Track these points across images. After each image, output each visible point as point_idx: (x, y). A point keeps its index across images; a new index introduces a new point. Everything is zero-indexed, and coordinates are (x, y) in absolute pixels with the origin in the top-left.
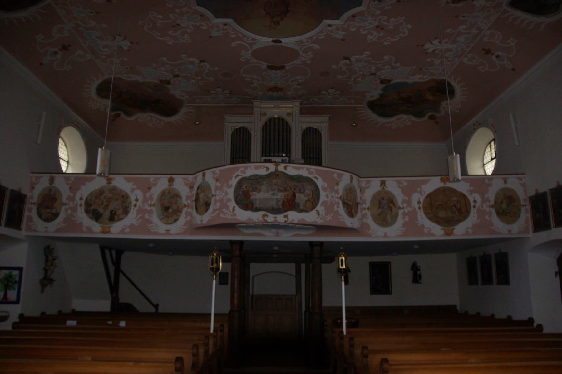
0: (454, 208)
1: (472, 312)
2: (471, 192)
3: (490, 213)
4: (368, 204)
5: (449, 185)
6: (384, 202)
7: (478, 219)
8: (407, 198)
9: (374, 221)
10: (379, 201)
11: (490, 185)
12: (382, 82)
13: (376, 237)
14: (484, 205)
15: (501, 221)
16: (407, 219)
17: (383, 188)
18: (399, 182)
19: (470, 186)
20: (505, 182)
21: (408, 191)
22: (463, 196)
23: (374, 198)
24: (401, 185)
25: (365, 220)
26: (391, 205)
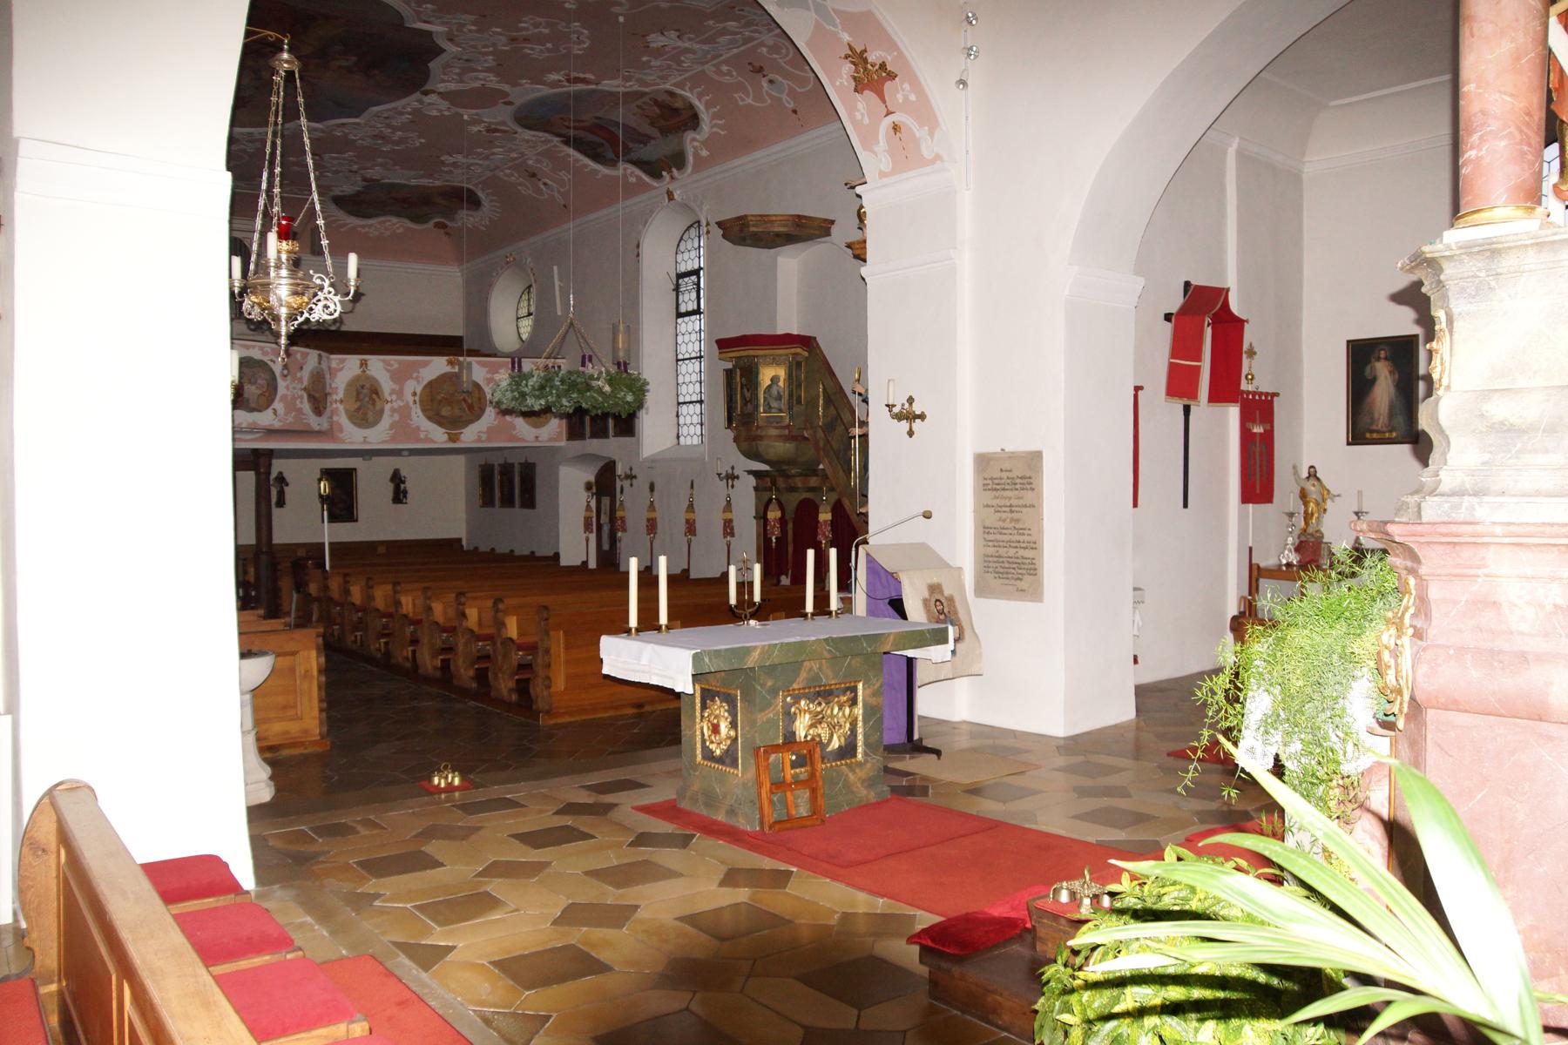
1: (483, 548)
4: (340, 395)
8: (397, 387)
12: (365, 180)
16: (396, 417)
18: (387, 363)
21: (399, 377)
23: (350, 385)
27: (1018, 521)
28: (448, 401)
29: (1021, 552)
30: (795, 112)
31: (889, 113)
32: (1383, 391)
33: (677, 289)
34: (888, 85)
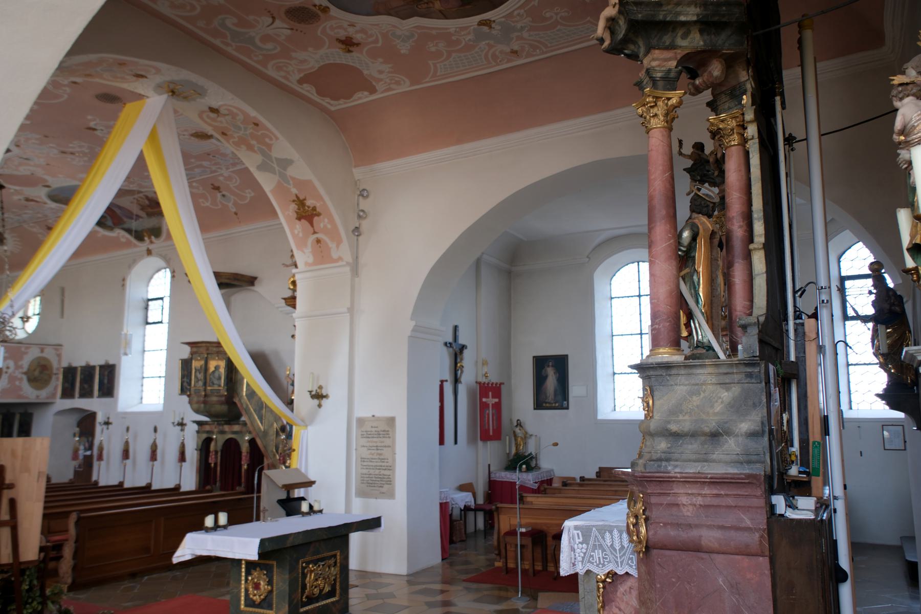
3: (21, 380)
11: (26, 353)
20: (42, 351)
27: (380, 454)
29: (383, 472)
30: (236, 214)
31: (315, 233)
32: (551, 382)
33: (147, 308)
34: (316, 218)
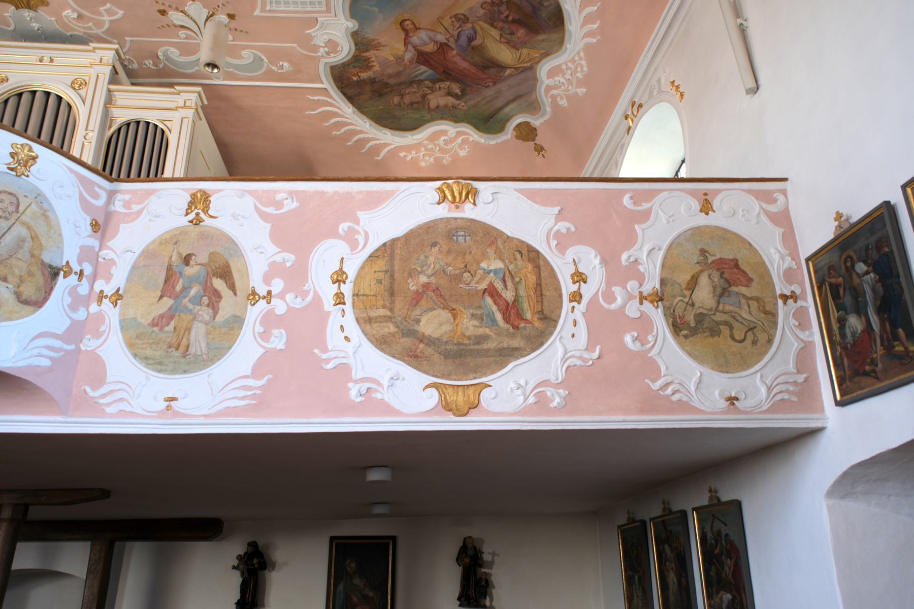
0: (489, 300)
2: (563, 242)
3: (643, 325)
4: (119, 278)
5: (468, 211)
6: (190, 271)
7: (589, 348)
9: (130, 345)
10: (169, 268)
11: (645, 216)
13: (122, 413)
14: (617, 290)
15: (690, 354)
16: (278, 340)
17: (197, 222)
19: (560, 216)
20: (706, 207)
21: (297, 237)
22: (533, 256)
23: (148, 254)
24: (270, 210)
25: (88, 344)
26: (219, 284)
28: (440, 294)
